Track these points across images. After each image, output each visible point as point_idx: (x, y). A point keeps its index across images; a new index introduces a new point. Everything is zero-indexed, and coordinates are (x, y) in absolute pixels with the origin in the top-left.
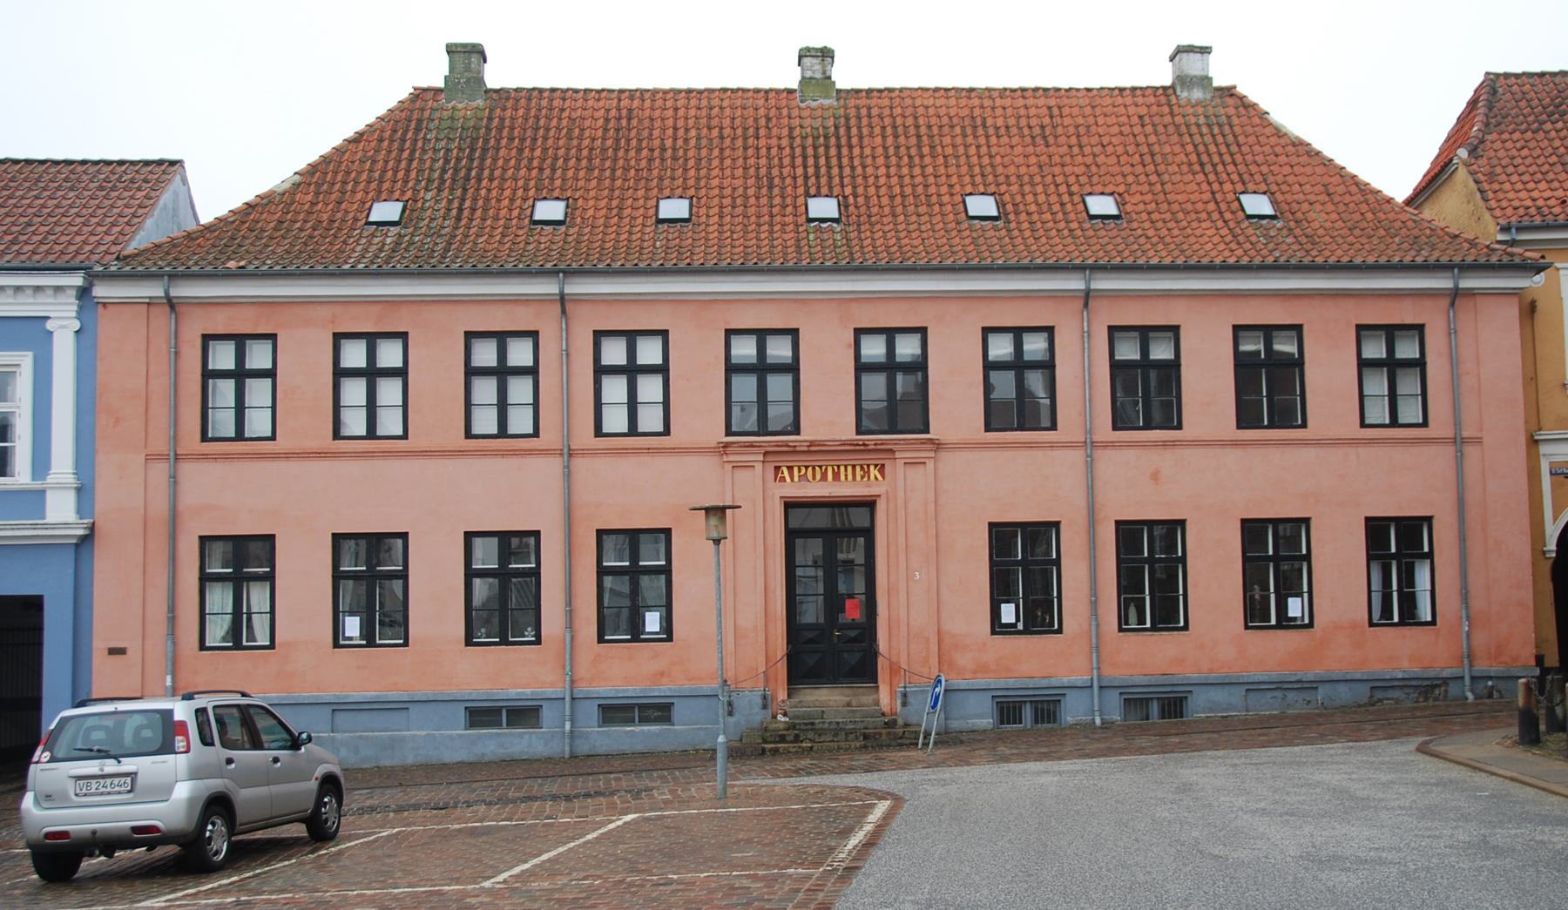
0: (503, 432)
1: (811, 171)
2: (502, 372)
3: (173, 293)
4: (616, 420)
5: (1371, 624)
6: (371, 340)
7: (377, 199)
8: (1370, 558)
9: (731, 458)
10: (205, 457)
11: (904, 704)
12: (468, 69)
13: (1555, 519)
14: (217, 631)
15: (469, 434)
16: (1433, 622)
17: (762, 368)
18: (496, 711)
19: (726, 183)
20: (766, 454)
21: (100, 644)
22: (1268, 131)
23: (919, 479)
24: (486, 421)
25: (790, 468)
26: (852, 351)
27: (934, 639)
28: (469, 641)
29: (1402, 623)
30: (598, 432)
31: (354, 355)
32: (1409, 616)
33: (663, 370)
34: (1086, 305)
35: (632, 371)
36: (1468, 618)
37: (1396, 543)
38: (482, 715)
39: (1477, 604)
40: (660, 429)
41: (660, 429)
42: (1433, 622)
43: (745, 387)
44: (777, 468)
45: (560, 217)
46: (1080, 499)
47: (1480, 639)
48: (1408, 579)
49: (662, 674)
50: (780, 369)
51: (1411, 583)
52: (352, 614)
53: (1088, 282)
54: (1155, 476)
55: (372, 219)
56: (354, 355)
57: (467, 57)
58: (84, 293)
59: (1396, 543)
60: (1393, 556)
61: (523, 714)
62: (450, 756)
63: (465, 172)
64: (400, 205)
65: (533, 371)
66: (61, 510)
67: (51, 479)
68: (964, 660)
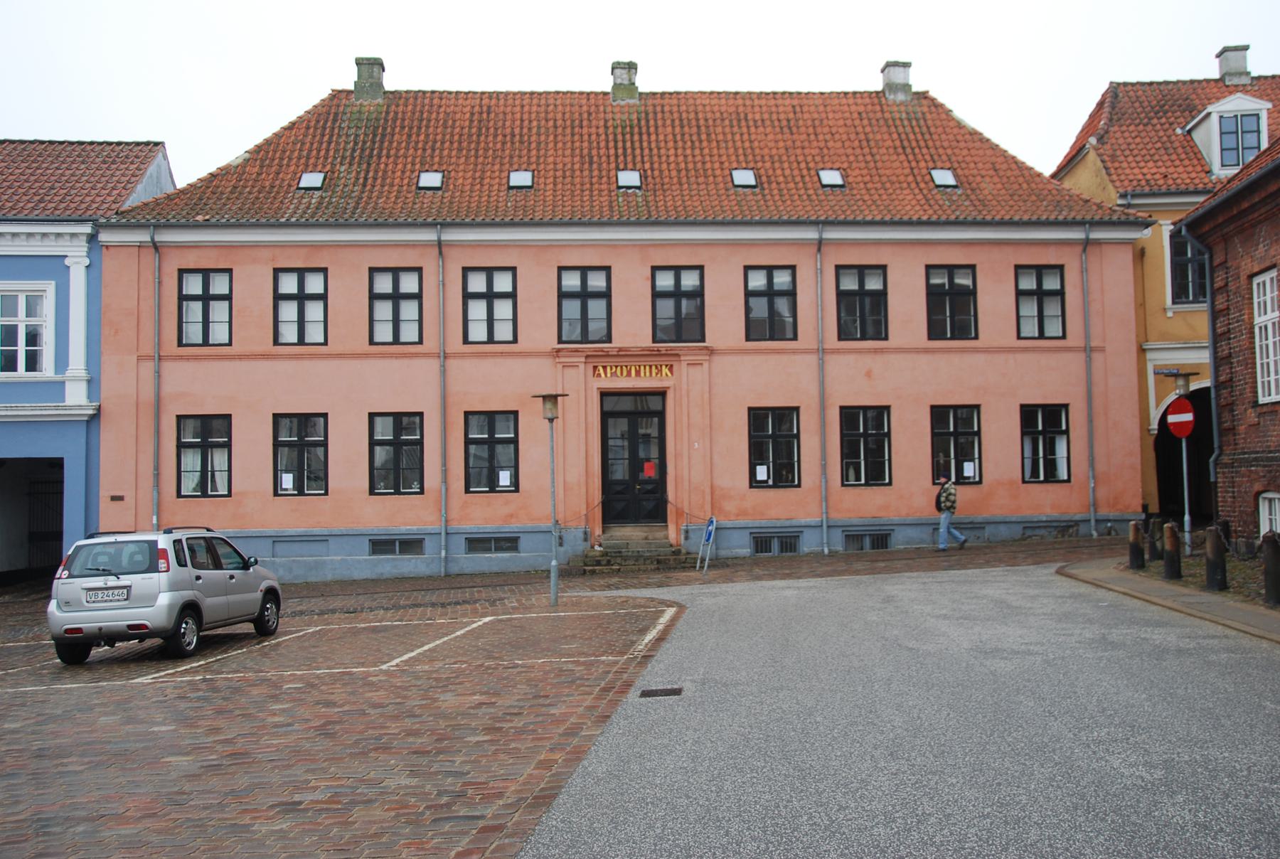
0: (396, 340)
1: (620, 151)
2: (396, 297)
3: (157, 238)
4: (478, 332)
5: (1024, 482)
6: (301, 273)
7: (305, 171)
8: (1023, 434)
9: (562, 360)
10: (181, 358)
11: (687, 538)
12: (371, 76)
13: (1157, 406)
14: (190, 484)
15: (372, 342)
16: (1068, 481)
17: (584, 295)
18: (392, 542)
19: (558, 160)
20: (587, 357)
21: (105, 493)
23: (698, 374)
24: (384, 333)
25: (604, 368)
26: (649, 283)
27: (708, 491)
28: (372, 492)
29: (1046, 481)
30: (466, 340)
31: (289, 285)
32: (1051, 476)
33: (512, 296)
34: (819, 250)
35: (490, 296)
36: (1094, 477)
37: (1043, 423)
38: (381, 545)
39: (1101, 467)
40: (511, 339)
41: (511, 339)
42: (1068, 481)
43: (572, 308)
44: (595, 368)
45: (438, 184)
46: (814, 390)
47: (1102, 493)
48: (1050, 449)
49: (512, 516)
50: (597, 295)
51: (1053, 453)
52: (287, 471)
53: (820, 233)
54: (869, 374)
55: (301, 185)
56: (289, 285)
57: (370, 67)
58: (92, 238)
59: (1043, 423)
60: (1040, 433)
61: (411, 545)
62: (358, 575)
63: (372, 153)
64: (322, 176)
65: (418, 297)
66: (76, 397)
67: (69, 373)
68: (730, 506)
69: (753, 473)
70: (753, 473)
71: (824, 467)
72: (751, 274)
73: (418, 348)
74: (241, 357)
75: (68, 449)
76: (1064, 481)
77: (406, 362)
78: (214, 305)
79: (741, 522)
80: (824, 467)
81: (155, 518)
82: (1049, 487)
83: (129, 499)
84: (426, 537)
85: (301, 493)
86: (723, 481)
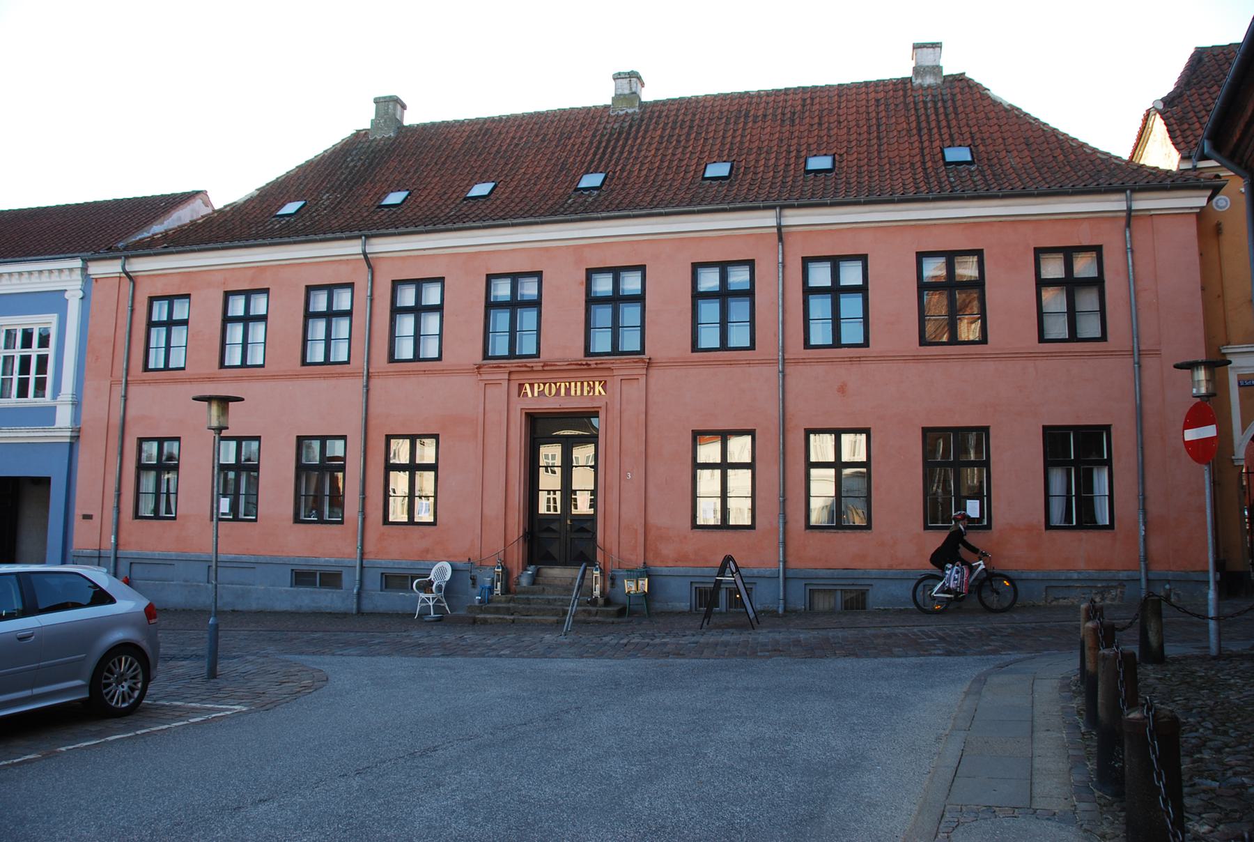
4: (405, 350)
5: (1048, 526)
8: (1048, 464)
9: (485, 377)
10: (144, 382)
11: (613, 584)
14: (147, 508)
16: (1111, 526)
17: (515, 305)
18: (312, 574)
20: (510, 373)
21: (78, 511)
22: (985, 103)
23: (634, 392)
25: (532, 385)
26: (583, 289)
27: (641, 531)
28: (297, 520)
29: (1080, 527)
31: (237, 307)
32: (1087, 521)
35: (419, 310)
36: (1145, 524)
37: (1075, 449)
38: (302, 577)
39: (1153, 509)
42: (1111, 526)
43: (502, 319)
44: (521, 386)
46: (774, 411)
47: (1156, 544)
48: (1086, 483)
49: (427, 551)
51: (1090, 488)
52: (225, 496)
54: (842, 389)
58: (84, 269)
59: (1075, 449)
60: (1072, 463)
61: (331, 579)
62: (280, 606)
66: (64, 417)
67: (59, 399)
68: (668, 550)
69: (214, 505)
70: (214, 505)
71: (119, 495)
72: (156, 305)
73: (346, 368)
74: (274, 377)
75: (55, 470)
76: (1104, 527)
77: (333, 382)
78: (175, 330)
79: (682, 570)
80: (119, 495)
81: (113, 538)
82: (1083, 535)
83: (97, 519)
84: (345, 571)
85: (236, 518)
86: (659, 519)
